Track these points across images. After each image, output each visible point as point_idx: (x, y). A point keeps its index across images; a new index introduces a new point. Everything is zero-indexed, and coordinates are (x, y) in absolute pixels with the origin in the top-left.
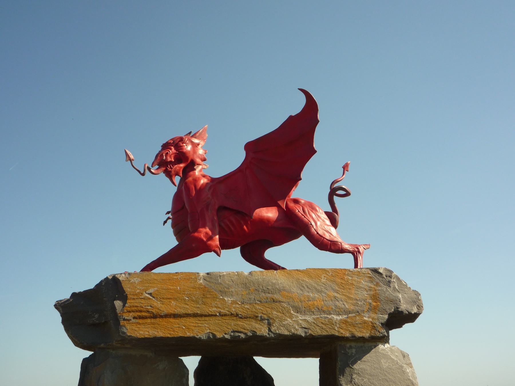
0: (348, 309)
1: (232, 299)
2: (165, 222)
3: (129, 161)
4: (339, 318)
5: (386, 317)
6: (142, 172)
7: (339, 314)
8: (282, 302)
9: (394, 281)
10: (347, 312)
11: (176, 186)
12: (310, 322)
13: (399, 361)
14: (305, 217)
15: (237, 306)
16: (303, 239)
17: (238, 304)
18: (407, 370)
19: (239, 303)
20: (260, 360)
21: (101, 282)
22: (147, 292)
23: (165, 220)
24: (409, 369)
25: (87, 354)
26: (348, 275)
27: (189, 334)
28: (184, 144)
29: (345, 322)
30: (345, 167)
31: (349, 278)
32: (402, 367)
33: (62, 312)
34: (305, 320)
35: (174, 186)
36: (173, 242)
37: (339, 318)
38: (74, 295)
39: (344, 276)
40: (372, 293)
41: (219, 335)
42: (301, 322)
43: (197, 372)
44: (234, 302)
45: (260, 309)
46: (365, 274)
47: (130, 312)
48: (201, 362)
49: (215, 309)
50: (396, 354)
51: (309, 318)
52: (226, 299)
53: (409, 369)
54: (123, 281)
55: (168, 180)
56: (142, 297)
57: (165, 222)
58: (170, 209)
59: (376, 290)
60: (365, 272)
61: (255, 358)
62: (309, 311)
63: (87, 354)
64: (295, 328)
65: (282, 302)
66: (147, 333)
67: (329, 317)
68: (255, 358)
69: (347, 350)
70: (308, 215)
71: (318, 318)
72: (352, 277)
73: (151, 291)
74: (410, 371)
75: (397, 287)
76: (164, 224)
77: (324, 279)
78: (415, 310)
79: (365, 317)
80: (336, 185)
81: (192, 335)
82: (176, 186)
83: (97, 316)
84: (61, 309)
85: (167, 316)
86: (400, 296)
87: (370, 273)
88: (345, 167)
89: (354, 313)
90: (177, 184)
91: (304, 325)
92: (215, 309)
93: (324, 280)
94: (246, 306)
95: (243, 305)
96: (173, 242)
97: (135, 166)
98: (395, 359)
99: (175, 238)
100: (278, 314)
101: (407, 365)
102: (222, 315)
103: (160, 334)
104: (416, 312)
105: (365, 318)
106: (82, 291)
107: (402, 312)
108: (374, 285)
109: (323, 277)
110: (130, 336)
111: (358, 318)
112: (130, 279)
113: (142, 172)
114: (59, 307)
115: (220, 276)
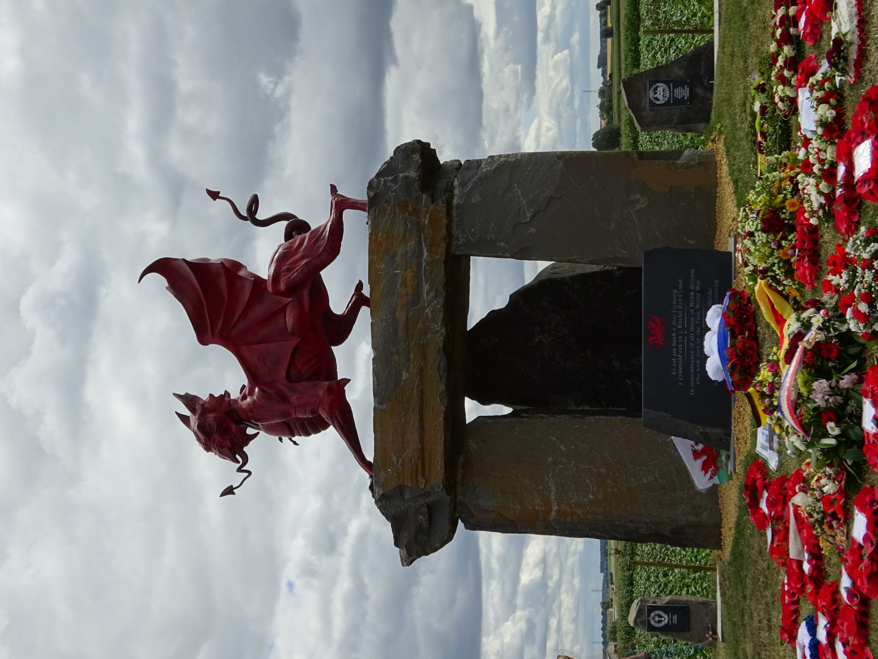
0: (416, 242)
1: (404, 372)
2: (295, 443)
3: (234, 491)
4: (426, 254)
5: (424, 196)
6: (247, 474)
7: (422, 254)
8: (407, 316)
9: (383, 180)
10: (419, 243)
11: (259, 433)
12: (429, 287)
13: (474, 179)
14: (297, 271)
15: (411, 366)
16: (323, 273)
17: (409, 366)
18: (483, 172)
19: (408, 364)
20: (472, 321)
21: (383, 514)
22: (396, 463)
23: (292, 443)
24: (483, 169)
25: (460, 525)
26: (376, 236)
27: (441, 419)
28: (207, 424)
29: (430, 246)
30: (214, 195)
31: (380, 235)
32: (480, 177)
33: (415, 556)
34: (427, 295)
35: (259, 435)
36: (331, 434)
37: (426, 254)
38: (397, 544)
39: (378, 241)
40: (397, 210)
41: (443, 387)
42: (429, 298)
43: (484, 401)
44: (408, 371)
45: (415, 343)
46: (375, 216)
47: (417, 481)
48: (472, 398)
49: (415, 392)
50: (466, 179)
51: (426, 288)
52: (404, 378)
53: (483, 169)
54: (383, 490)
55: (251, 443)
56: (401, 469)
57: (295, 443)
58: (277, 438)
59: (394, 205)
60: (372, 215)
61: (469, 328)
62: (418, 288)
63: (460, 525)
64: (436, 305)
65: (407, 316)
66: (440, 463)
67: (424, 265)
68: (469, 328)
69: (460, 243)
70: (294, 266)
71: (425, 277)
72: (379, 233)
73: (395, 459)
74: (486, 168)
75: (391, 178)
76: (297, 445)
77: (381, 265)
78: (417, 157)
79: (424, 222)
80: (244, 213)
81: (442, 416)
82: (259, 433)
83: (421, 517)
84: (413, 558)
85: (422, 440)
86: (401, 175)
87: (374, 209)
88: (214, 195)
89: (420, 234)
90: (257, 431)
91: (432, 294)
92: (415, 392)
93: (383, 265)
94: (412, 357)
95: (411, 360)
96: (331, 434)
97: (245, 482)
98: (472, 184)
99: (323, 432)
100: (420, 322)
101: (479, 167)
102: (421, 382)
103: (440, 449)
104: (419, 156)
105: (427, 222)
106: (392, 535)
107: (419, 176)
108: (388, 205)
109: (379, 266)
110: (442, 480)
111: (426, 232)
112: (381, 482)
113: (247, 474)
114: (410, 560)
115: (378, 385)
